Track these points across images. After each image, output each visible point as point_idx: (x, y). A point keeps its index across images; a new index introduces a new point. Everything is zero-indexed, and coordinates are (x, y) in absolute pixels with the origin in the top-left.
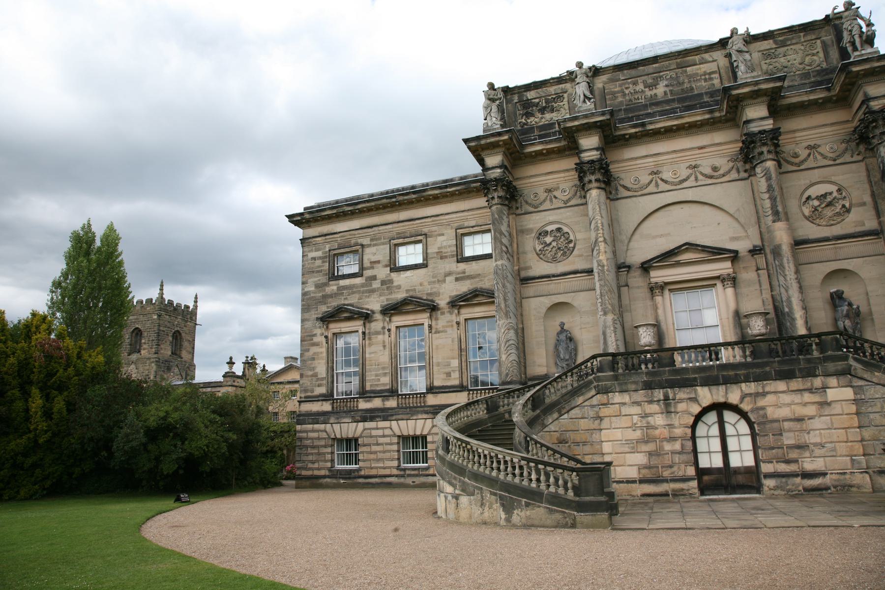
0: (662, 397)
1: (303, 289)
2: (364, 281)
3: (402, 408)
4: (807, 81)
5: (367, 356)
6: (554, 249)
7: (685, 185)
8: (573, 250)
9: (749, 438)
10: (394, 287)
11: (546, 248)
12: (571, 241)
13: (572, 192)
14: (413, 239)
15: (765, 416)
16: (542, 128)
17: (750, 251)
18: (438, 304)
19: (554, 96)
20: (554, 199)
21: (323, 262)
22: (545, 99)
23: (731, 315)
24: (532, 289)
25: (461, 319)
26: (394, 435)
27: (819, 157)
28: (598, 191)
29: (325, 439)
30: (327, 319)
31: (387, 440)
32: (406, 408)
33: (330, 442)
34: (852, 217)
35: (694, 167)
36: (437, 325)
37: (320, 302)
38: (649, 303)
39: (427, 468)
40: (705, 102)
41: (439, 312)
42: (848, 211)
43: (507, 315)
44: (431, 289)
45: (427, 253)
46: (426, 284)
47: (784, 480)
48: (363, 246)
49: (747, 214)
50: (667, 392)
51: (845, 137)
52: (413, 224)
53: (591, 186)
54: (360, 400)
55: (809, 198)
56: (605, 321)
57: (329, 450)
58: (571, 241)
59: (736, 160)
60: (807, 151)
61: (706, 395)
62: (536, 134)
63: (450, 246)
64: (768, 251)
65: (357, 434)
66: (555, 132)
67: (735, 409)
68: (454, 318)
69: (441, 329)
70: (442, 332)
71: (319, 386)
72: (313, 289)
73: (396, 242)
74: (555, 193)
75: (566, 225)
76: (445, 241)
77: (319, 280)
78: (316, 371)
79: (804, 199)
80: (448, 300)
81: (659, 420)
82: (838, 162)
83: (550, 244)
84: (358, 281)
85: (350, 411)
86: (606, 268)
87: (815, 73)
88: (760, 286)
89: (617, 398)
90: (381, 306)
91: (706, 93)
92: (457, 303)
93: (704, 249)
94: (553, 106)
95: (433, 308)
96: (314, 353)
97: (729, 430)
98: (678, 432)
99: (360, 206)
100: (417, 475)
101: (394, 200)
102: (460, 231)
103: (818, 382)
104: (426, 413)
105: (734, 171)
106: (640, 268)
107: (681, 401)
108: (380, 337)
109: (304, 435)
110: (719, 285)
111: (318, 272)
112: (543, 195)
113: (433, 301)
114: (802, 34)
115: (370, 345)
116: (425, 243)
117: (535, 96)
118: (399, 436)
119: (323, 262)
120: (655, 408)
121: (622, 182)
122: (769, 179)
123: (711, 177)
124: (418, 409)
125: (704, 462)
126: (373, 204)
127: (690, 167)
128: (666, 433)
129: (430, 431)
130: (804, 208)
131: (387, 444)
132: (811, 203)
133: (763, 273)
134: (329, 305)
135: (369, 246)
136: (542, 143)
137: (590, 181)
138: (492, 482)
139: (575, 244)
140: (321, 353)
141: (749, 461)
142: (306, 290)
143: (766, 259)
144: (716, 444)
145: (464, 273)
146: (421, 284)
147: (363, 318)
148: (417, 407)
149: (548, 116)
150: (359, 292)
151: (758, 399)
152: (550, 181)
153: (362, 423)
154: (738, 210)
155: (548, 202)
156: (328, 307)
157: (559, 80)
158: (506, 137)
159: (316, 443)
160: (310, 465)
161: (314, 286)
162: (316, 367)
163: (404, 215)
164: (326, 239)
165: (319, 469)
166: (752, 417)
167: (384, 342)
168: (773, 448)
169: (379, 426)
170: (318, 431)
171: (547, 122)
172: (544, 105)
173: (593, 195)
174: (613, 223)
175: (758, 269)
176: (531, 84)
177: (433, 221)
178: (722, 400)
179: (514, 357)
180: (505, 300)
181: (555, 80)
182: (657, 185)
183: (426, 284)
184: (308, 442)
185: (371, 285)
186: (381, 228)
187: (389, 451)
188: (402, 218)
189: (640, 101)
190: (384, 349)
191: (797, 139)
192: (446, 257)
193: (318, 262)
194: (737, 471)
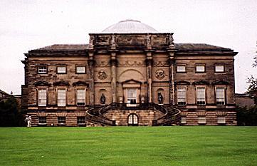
24: (97, 85)
76: (72, 67)
81: (123, 115)
92: (74, 85)
138: (100, 122)
152: (103, 60)
163: (60, 59)
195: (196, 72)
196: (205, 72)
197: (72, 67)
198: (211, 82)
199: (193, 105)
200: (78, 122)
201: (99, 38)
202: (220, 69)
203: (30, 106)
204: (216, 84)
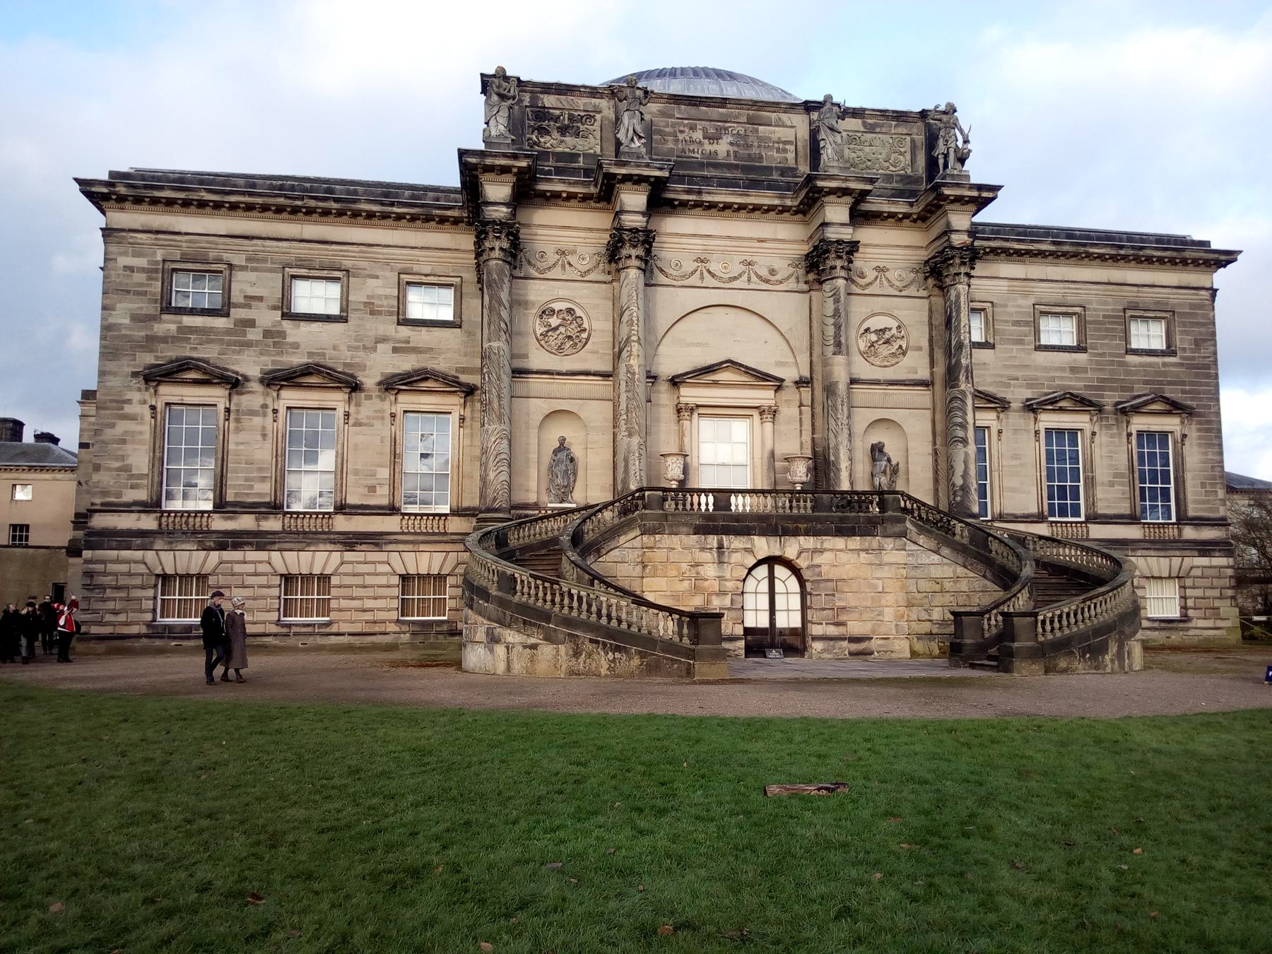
0: (715, 545)
1: (103, 319)
2: (232, 326)
3: (291, 533)
4: (887, 185)
5: (231, 447)
6: (561, 337)
7: (735, 284)
8: (586, 343)
9: (798, 597)
10: (288, 343)
11: (550, 333)
12: (585, 330)
13: (593, 263)
14: (324, 274)
15: (820, 574)
16: (560, 156)
17: (796, 383)
18: (362, 383)
19: (582, 114)
20: (567, 266)
21: (150, 278)
22: (569, 114)
23: (766, 455)
25: (399, 409)
26: (275, 574)
27: (885, 283)
28: (638, 272)
29: (142, 575)
30: (155, 376)
31: (263, 580)
32: (298, 533)
33: (152, 580)
34: (907, 361)
35: (749, 264)
36: (358, 413)
37: (141, 347)
38: (674, 427)
39: (329, 624)
40: (773, 180)
41: (363, 395)
42: (904, 354)
43: (500, 418)
44: (352, 357)
45: (347, 301)
46: (343, 348)
47: (831, 643)
48: (231, 267)
49: (800, 339)
50: (722, 540)
51: (915, 266)
52: (328, 250)
53: (629, 262)
54: (215, 516)
55: (867, 330)
56: (629, 445)
57: (150, 593)
58: (585, 330)
59: (797, 266)
60: (875, 273)
61: (764, 546)
62: (550, 163)
63: (387, 297)
64: (818, 385)
65: (208, 568)
66: (579, 169)
67: (789, 564)
68: (387, 406)
69: (365, 421)
70: (365, 425)
71: (132, 487)
72: (127, 321)
73: (294, 271)
74: (570, 258)
75: (581, 307)
76: (380, 287)
77: (141, 308)
78: (127, 462)
79: (862, 331)
80: (378, 379)
81: (710, 571)
82: (903, 293)
83: (556, 329)
84: (220, 322)
85: (195, 533)
86: (637, 376)
87: (898, 178)
88: (801, 426)
89: (666, 540)
90: (262, 371)
91: (777, 168)
92: (393, 384)
93: (748, 370)
94: (578, 128)
95: (354, 387)
96: (126, 432)
97: (779, 587)
98: (730, 585)
99: (233, 199)
100: (310, 634)
101: (299, 203)
102: (406, 278)
103: (874, 542)
104: (333, 542)
105: (793, 279)
106: (668, 381)
107: (736, 551)
108: (257, 420)
109: (100, 567)
110: (755, 413)
111: (138, 293)
112: (552, 258)
113: (352, 376)
114: (894, 123)
115: (238, 430)
116: (345, 285)
117: (554, 106)
118: (158, 576)
119: (150, 278)
120: (707, 556)
121: (658, 263)
122: (837, 301)
123: (767, 281)
124: (318, 536)
125: (750, 623)
126: (259, 200)
127: (744, 262)
128: (715, 586)
129: (337, 569)
130: (860, 341)
131: (260, 586)
132: (868, 335)
133: (807, 410)
134: (159, 354)
135: (243, 268)
136: (563, 182)
137: (630, 257)
139: (589, 335)
140: (141, 433)
141: (796, 622)
142: (111, 320)
143: (812, 394)
144: (764, 602)
145: (408, 342)
146: (335, 348)
147: (229, 386)
148: (316, 533)
149: (570, 140)
150: (221, 342)
151: (815, 555)
152: (568, 239)
153: (217, 552)
154: (790, 329)
155: (558, 268)
156: (157, 358)
157: (593, 92)
158: (523, 164)
159: (123, 581)
160: (109, 618)
161: (128, 316)
162: (128, 456)
164: (156, 239)
165: (127, 624)
166: (806, 575)
167: (264, 428)
168: (824, 609)
169: (247, 559)
170: (128, 562)
171: (568, 150)
172: (566, 122)
173: (631, 277)
174: (648, 317)
175: (801, 405)
176: (552, 84)
177: (361, 252)
178: (777, 553)
179: (504, 476)
180: (499, 397)
181: (588, 90)
182: (702, 278)
183: (343, 348)
184: (107, 580)
185: (245, 335)
186: (268, 243)
187: (264, 598)
188: (306, 236)
189: (696, 155)
190: (264, 440)
191: (868, 256)
192: (380, 313)
193: (139, 277)
194: (782, 632)
195: (1040, 348)
196: (1080, 349)
197: (380, 287)
198: (1109, 399)
199: (1027, 519)
200: (405, 607)
201: (542, 114)
202: (1149, 336)
203: (110, 508)
204: (1136, 410)
